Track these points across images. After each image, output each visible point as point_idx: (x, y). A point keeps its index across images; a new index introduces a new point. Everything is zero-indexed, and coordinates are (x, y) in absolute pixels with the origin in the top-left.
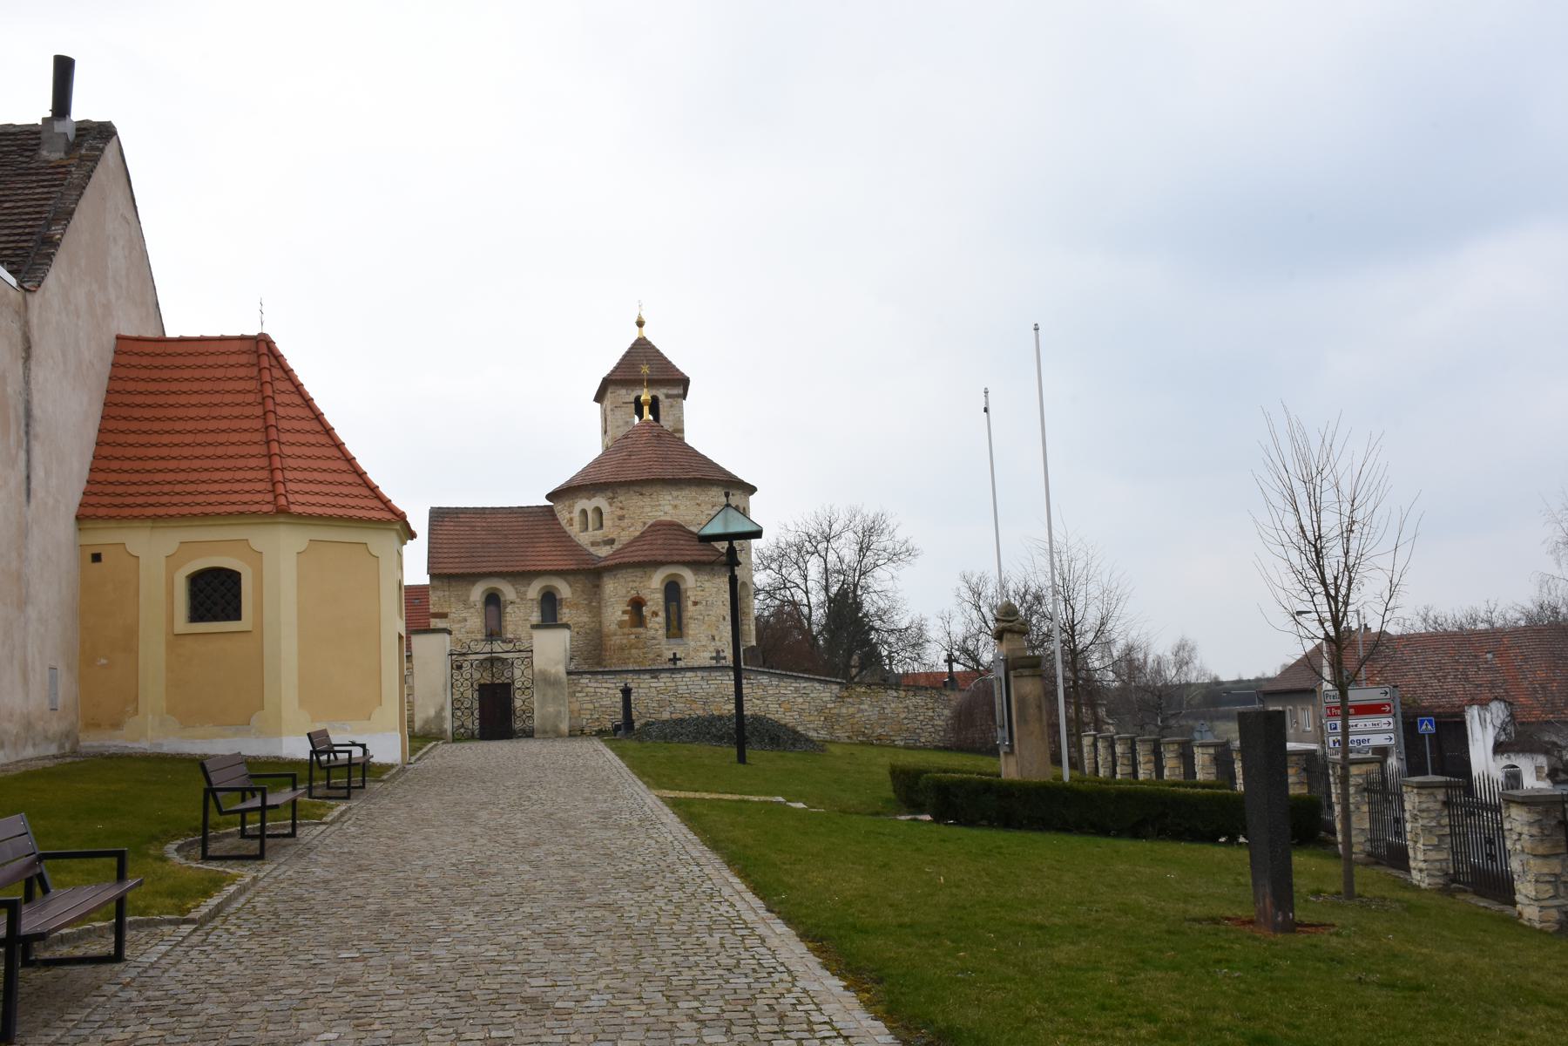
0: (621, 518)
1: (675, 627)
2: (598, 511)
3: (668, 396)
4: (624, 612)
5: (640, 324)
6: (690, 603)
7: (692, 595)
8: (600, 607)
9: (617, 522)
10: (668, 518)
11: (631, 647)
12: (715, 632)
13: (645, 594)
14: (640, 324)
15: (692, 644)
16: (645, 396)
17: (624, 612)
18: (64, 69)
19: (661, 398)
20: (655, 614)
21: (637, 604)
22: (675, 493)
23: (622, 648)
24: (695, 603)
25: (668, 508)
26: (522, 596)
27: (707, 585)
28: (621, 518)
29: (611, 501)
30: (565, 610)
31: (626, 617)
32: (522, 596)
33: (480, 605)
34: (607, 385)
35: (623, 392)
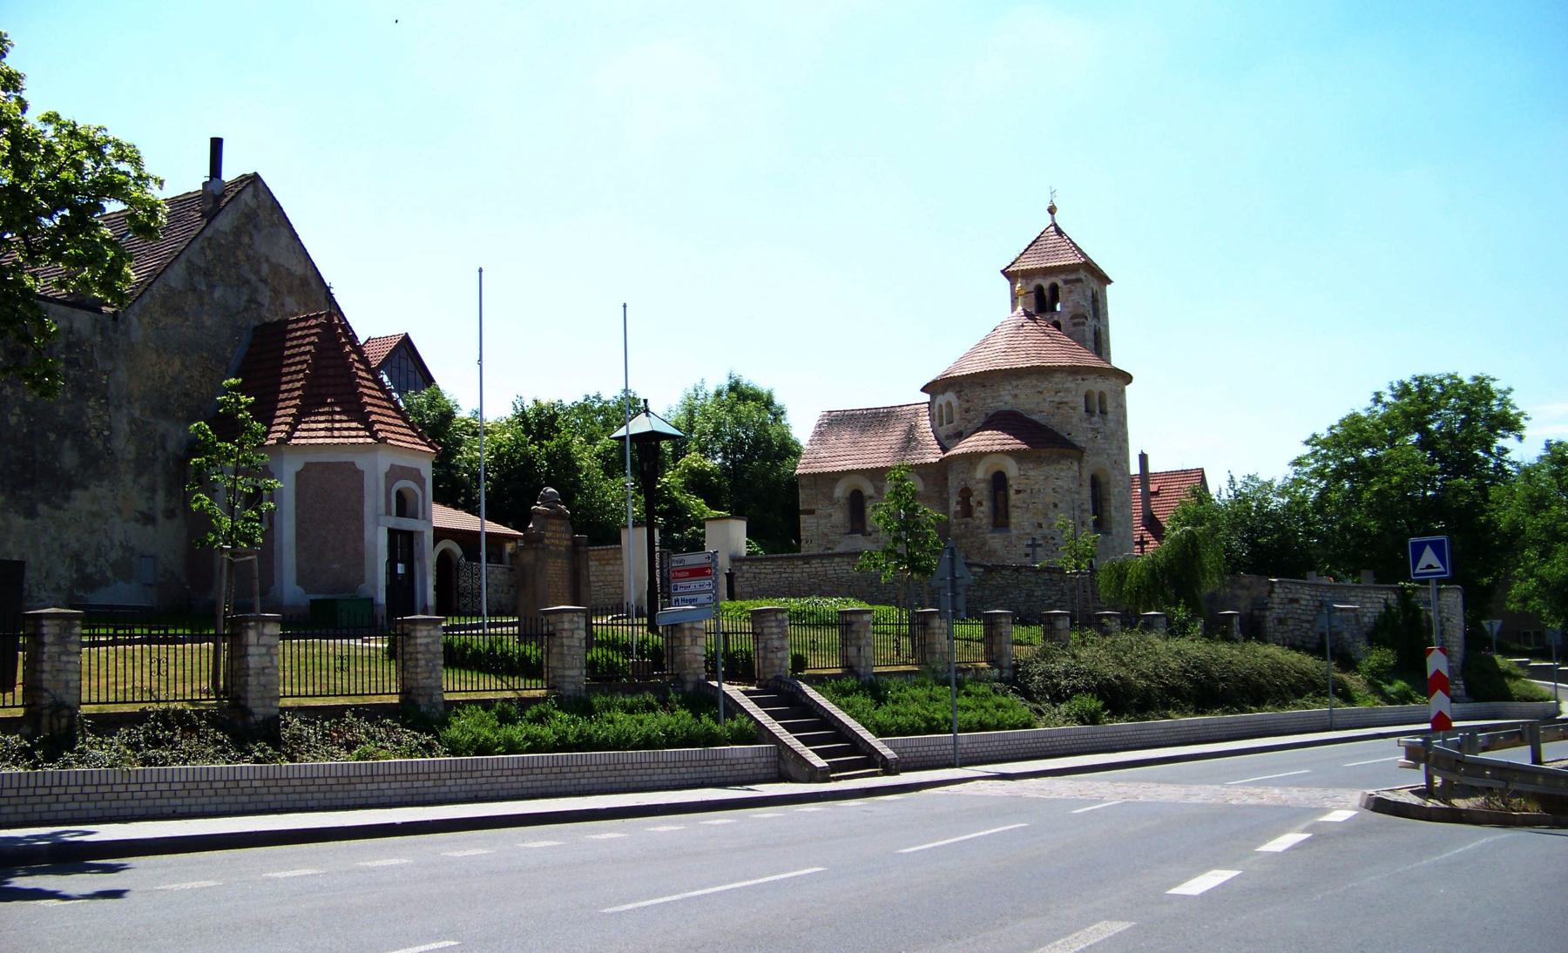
1: (1000, 518)
2: (949, 404)
3: (1066, 282)
5: (1052, 210)
6: (1012, 492)
7: (1014, 485)
8: (947, 500)
10: (1008, 408)
12: (1041, 520)
13: (971, 485)
14: (1052, 210)
15: (1014, 532)
16: (1046, 284)
18: (217, 145)
19: (1060, 284)
21: (966, 493)
24: (1018, 492)
25: (1008, 398)
27: (1032, 473)
29: (959, 394)
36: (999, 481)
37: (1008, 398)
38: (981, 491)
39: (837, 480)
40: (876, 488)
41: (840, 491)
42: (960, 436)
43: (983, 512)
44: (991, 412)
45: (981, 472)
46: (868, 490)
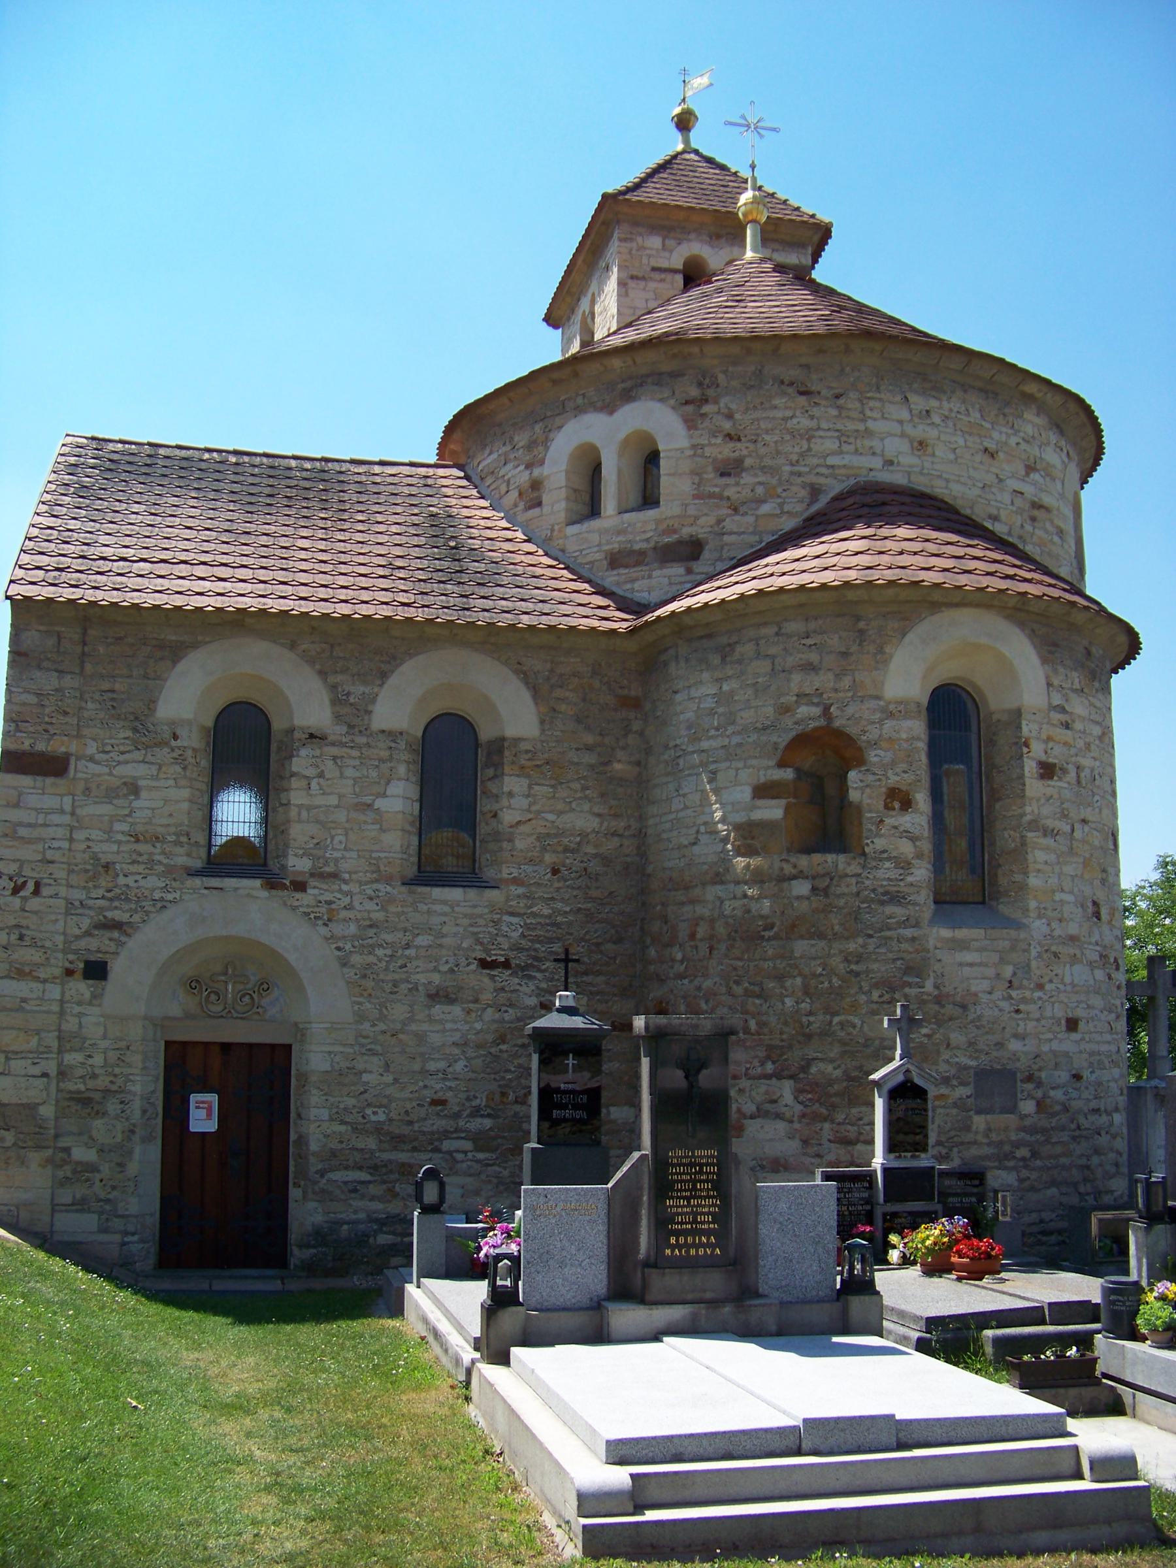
0: (729, 469)
4: (763, 791)
5: (684, 122)
6: (1030, 767)
9: (714, 483)
10: (897, 478)
11: (792, 930)
14: (684, 122)
15: (1038, 927)
17: (763, 791)
20: (900, 799)
22: (919, 402)
23: (750, 933)
24: (1048, 771)
26: (352, 713)
28: (729, 469)
29: (692, 411)
30: (512, 783)
31: (773, 811)
32: (352, 713)
33: (192, 740)
34: (614, 215)
35: (655, 242)
36: (953, 713)
37: (895, 447)
38: (896, 747)
39: (176, 653)
40: (338, 700)
41: (188, 696)
42: (688, 554)
43: (901, 843)
44: (836, 488)
45: (907, 674)
46: (305, 702)
